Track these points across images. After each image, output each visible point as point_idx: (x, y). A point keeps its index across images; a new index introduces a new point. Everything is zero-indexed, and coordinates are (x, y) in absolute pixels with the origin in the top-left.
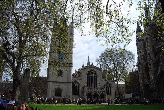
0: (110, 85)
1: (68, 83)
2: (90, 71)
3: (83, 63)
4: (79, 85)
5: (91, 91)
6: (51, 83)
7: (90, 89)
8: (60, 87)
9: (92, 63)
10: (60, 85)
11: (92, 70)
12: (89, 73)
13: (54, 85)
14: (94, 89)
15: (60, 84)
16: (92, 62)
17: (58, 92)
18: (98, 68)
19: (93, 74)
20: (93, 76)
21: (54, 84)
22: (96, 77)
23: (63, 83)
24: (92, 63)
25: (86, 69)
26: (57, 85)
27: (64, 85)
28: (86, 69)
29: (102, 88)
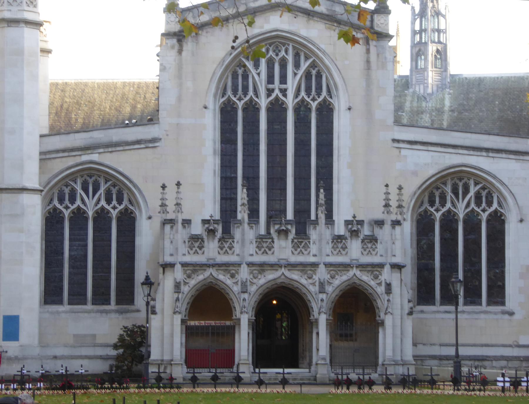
5: (225, 266)
19: (291, 85)
20: (290, 102)
29: (355, 233)
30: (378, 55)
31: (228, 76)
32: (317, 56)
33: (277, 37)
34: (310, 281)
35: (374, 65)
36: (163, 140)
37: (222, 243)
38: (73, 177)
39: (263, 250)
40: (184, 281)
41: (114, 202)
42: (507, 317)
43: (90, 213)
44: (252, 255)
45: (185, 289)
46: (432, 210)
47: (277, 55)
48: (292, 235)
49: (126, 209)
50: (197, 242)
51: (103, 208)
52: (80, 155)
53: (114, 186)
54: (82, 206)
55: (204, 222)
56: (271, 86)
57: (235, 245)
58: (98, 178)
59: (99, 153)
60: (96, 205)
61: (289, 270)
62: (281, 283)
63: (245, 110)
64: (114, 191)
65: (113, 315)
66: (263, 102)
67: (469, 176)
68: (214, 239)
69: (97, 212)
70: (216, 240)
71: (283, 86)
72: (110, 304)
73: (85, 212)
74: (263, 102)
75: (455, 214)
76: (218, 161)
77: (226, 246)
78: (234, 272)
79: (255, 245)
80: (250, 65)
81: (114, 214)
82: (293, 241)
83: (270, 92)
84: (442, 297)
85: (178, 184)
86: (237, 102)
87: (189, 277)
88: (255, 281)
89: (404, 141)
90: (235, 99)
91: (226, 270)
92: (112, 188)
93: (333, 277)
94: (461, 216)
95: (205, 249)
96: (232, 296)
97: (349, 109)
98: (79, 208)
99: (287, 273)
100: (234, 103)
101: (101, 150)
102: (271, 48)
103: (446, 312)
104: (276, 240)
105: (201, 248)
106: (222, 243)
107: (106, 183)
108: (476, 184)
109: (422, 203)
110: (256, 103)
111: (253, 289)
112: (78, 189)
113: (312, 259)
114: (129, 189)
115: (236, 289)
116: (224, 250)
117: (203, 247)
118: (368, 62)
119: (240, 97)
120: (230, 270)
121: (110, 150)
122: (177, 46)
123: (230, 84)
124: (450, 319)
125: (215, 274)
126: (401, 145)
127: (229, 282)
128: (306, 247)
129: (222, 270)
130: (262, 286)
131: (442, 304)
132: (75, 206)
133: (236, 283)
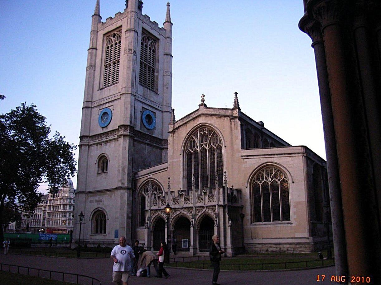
0: (279, 171)
2: (194, 132)
6: (84, 195)
9: (203, 101)
11: (201, 127)
12: (189, 141)
13: (91, 202)
16: (203, 96)
18: (222, 112)
22: (220, 149)
24: (203, 101)
25: (178, 128)
26: (96, 201)
27: (111, 197)
28: (181, 129)
30: (234, 124)
32: (214, 129)
33: (202, 126)
34: (191, 214)
35: (233, 129)
36: (169, 168)
42: (289, 225)
46: (258, 182)
52: (147, 176)
56: (202, 144)
59: (152, 175)
62: (181, 215)
64: (158, 187)
67: (272, 166)
71: (205, 143)
74: (198, 150)
75: (268, 183)
80: (194, 137)
82: (184, 199)
84: (274, 218)
89: (245, 156)
93: (199, 212)
94: (270, 184)
97: (225, 147)
101: (152, 174)
103: (265, 224)
104: (179, 199)
108: (275, 170)
109: (255, 180)
113: (191, 205)
118: (231, 128)
122: (173, 136)
123: (189, 145)
124: (266, 227)
126: (244, 158)
128: (189, 200)
131: (264, 221)
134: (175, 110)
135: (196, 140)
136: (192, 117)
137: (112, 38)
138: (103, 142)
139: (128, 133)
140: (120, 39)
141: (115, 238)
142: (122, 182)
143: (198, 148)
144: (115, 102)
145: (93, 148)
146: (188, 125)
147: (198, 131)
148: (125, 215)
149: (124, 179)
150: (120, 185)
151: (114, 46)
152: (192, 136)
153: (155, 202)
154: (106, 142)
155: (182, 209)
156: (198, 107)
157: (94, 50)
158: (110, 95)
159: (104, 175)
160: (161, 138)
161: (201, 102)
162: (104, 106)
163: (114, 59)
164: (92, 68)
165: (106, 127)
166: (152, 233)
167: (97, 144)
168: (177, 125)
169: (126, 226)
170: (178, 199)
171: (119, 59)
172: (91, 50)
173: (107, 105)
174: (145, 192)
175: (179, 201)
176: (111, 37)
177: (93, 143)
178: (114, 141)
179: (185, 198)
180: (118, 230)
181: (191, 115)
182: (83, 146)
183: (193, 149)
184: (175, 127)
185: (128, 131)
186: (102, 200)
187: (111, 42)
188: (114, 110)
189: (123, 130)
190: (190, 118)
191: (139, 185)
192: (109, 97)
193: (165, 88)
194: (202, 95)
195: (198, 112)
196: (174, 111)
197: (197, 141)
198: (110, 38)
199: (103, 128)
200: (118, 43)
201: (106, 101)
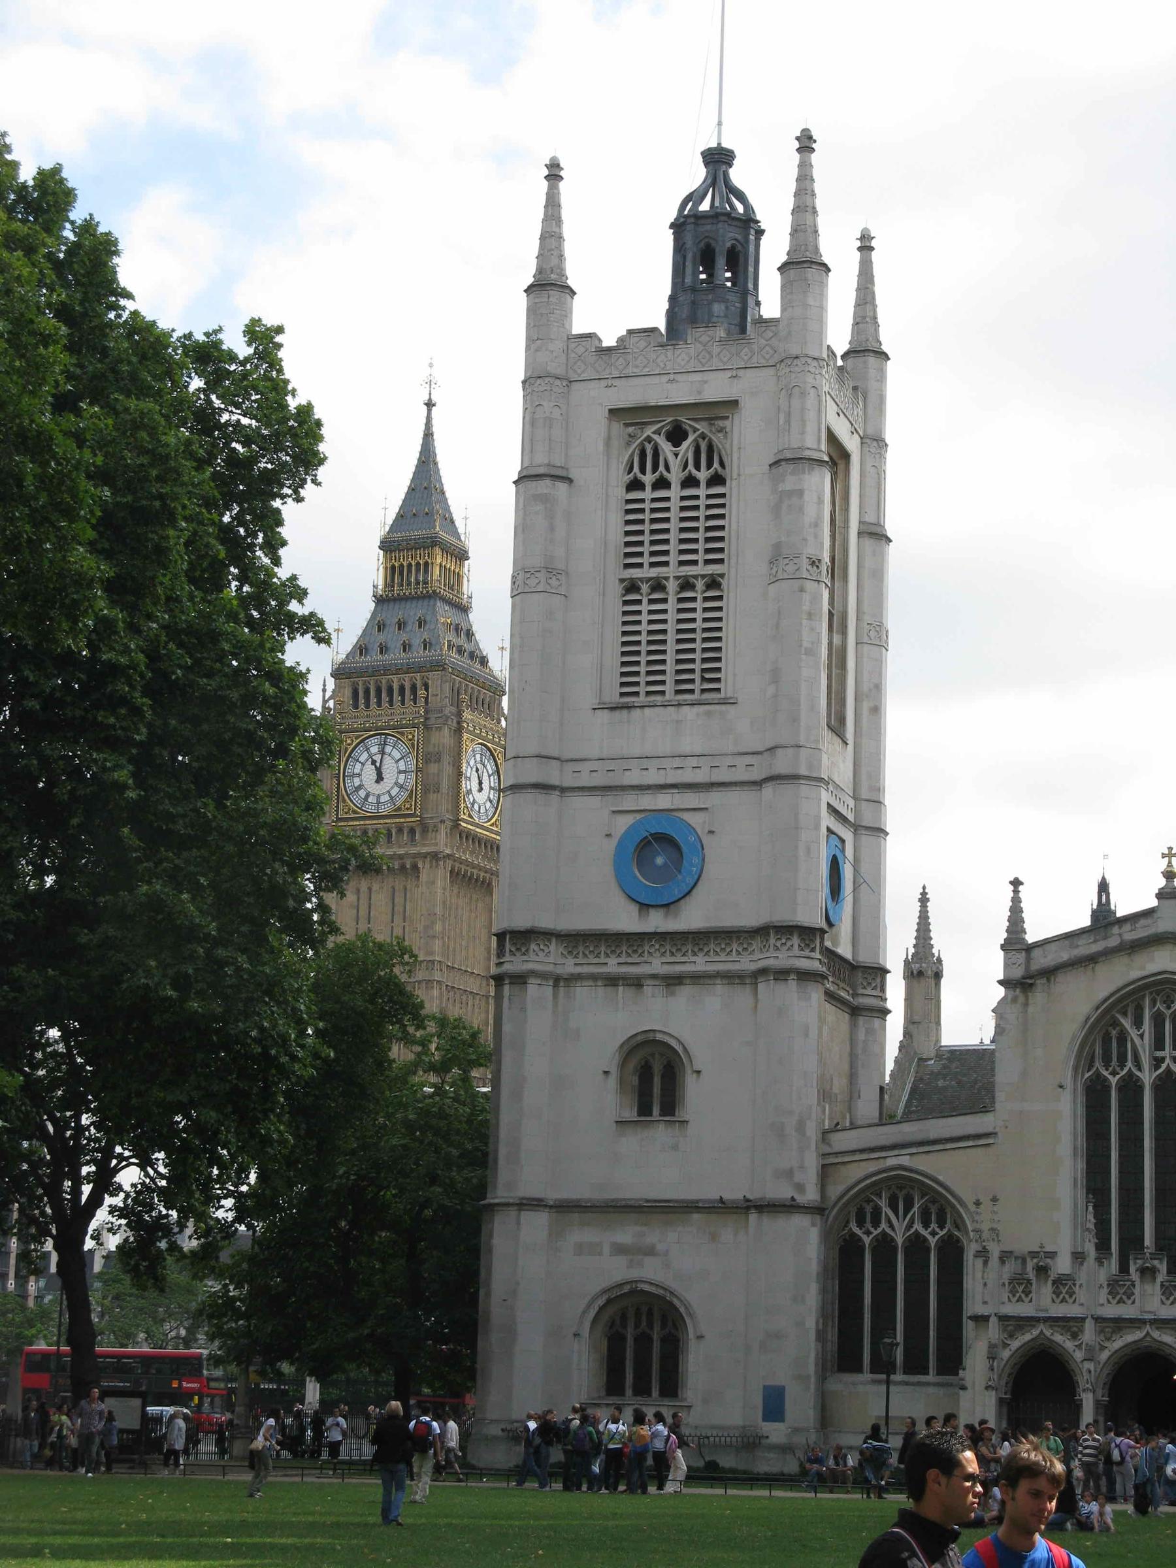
1: (753, 1217)
3: (1016, 883)
4: (959, 1224)
7: (1045, 1292)
8: (651, 1272)
10: (651, 1251)
13: (580, 1249)
14: (1118, 1288)
15: (653, 1236)
16: (1169, 855)
17: (643, 1341)
21: (581, 1234)
23: (696, 1216)
25: (1049, 973)
26: (620, 1250)
27: (714, 1237)
31: (1095, 1040)
37: (1057, 1287)
38: (875, 1188)
39: (1118, 1297)
40: (1004, 1343)
41: (934, 1225)
43: (900, 1241)
44: (1103, 1305)
45: (1006, 1354)
47: (1169, 1008)
48: (1162, 1277)
49: (950, 1235)
50: (1022, 1284)
51: (917, 1233)
53: (934, 1202)
54: (888, 1231)
55: (1034, 1254)
56: (1159, 1054)
57: (1077, 1289)
58: (911, 1192)
60: (909, 1230)
61: (1157, 1328)
62: (1146, 1347)
63: (1120, 1089)
64: (934, 1209)
65: (931, 1390)
66: (1147, 1077)
68: (1046, 1281)
69: (909, 1239)
70: (1050, 1283)
72: (928, 1374)
73: (893, 1240)
74: (1147, 1077)
76: (1081, 1165)
77: (1064, 1292)
78: (1075, 1329)
79: (1106, 1290)
80: (1127, 1023)
81: (933, 1241)
82: (1162, 1285)
83: (1158, 1062)
85: (995, 1200)
86: (1110, 1077)
87: (1011, 1336)
88: (1106, 1344)
90: (1106, 1073)
91: (1065, 1326)
92: (930, 1205)
95: (1033, 1295)
96: (1073, 1366)
98: (884, 1233)
99: (1156, 1334)
100: (1106, 1079)
101: (914, 1150)
102: (1159, 999)
104: (1138, 1283)
105: (1027, 1293)
106: (1057, 1287)
107: (922, 1198)
110: (1138, 1079)
111: (1105, 1355)
112: (883, 1205)
114: (953, 1207)
115: (1078, 1355)
116: (1061, 1297)
117: (1030, 1292)
119: (1114, 1069)
120: (1070, 1327)
121: (926, 1149)
123: (1098, 1051)
125: (1048, 1333)
127: (1069, 1345)
129: (1059, 1326)
130: (1116, 1351)
132: (879, 1230)
133: (1079, 1347)
134: (1022, 883)
135: (1133, 1033)
136: (1120, 935)
137: (666, 447)
138: (654, 977)
139: (815, 966)
140: (716, 465)
141: (764, 1420)
142: (796, 1180)
143: (1140, 1070)
144: (714, 798)
145: (582, 993)
146: (1099, 967)
147: (1144, 997)
148: (811, 1323)
149: (802, 1167)
150: (783, 1192)
151: (675, 492)
152: (1119, 1016)
153: (1021, 1289)
154: (672, 982)
155: (1151, 1324)
156: (1154, 903)
157: (562, 486)
158: (686, 749)
159: (661, 1134)
160: (848, 955)
161: (1162, 882)
162: (647, 801)
163: (681, 563)
164: (554, 582)
165: (667, 906)
166: (1005, 1410)
167: (612, 981)
168: (1041, 960)
169: (811, 1369)
170: (1134, 1286)
171: (722, 576)
172: (548, 482)
173: (664, 801)
174: (860, 1224)
175: (1137, 1291)
176: (655, 437)
177: (579, 970)
178: (718, 981)
179: (1167, 1284)
180: (783, 1388)
181: (1117, 927)
182: (532, 980)
183: (1118, 1069)
184: (1035, 966)
185: (813, 955)
186: (660, 1247)
187: (655, 468)
188: (711, 832)
189: (796, 947)
190: (1113, 942)
191: (841, 1188)
192: (677, 762)
193: (866, 706)
194: (1166, 852)
195: (1149, 921)
196: (1021, 888)
197: (1141, 1040)
198: (649, 439)
199: (644, 907)
200: (703, 484)
201: (653, 777)
